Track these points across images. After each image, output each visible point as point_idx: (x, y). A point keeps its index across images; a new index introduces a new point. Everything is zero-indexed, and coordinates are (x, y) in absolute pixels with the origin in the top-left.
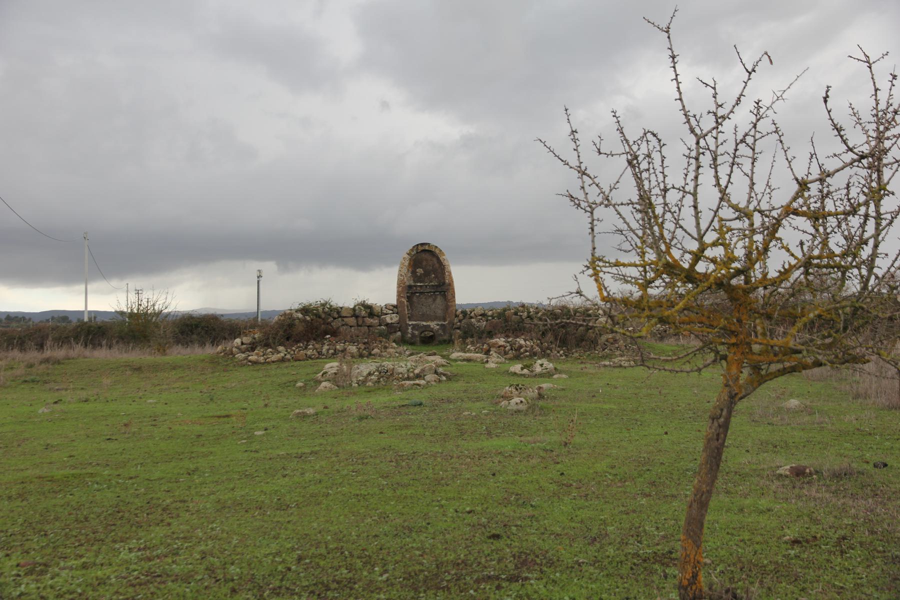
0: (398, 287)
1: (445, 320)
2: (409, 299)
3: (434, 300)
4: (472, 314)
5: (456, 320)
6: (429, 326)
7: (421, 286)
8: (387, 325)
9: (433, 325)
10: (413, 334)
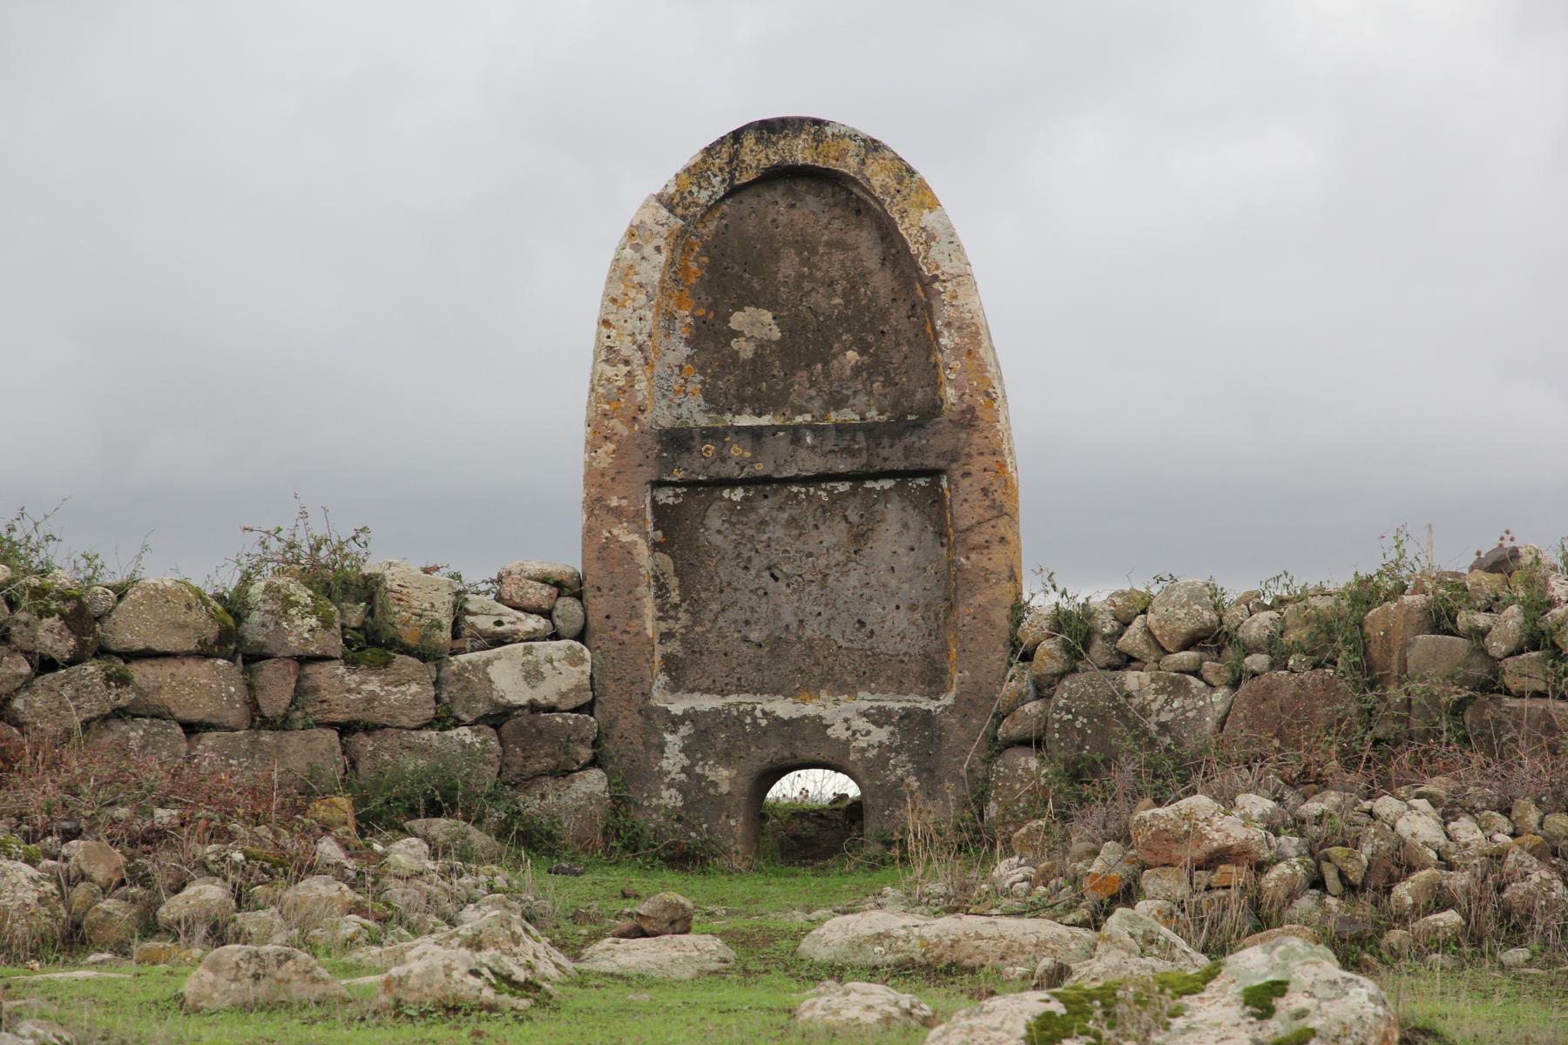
0: (598, 434)
1: (934, 680)
2: (672, 528)
3: (860, 538)
5: (1018, 681)
6: (819, 725)
7: (756, 434)
8: (499, 717)
10: (695, 789)
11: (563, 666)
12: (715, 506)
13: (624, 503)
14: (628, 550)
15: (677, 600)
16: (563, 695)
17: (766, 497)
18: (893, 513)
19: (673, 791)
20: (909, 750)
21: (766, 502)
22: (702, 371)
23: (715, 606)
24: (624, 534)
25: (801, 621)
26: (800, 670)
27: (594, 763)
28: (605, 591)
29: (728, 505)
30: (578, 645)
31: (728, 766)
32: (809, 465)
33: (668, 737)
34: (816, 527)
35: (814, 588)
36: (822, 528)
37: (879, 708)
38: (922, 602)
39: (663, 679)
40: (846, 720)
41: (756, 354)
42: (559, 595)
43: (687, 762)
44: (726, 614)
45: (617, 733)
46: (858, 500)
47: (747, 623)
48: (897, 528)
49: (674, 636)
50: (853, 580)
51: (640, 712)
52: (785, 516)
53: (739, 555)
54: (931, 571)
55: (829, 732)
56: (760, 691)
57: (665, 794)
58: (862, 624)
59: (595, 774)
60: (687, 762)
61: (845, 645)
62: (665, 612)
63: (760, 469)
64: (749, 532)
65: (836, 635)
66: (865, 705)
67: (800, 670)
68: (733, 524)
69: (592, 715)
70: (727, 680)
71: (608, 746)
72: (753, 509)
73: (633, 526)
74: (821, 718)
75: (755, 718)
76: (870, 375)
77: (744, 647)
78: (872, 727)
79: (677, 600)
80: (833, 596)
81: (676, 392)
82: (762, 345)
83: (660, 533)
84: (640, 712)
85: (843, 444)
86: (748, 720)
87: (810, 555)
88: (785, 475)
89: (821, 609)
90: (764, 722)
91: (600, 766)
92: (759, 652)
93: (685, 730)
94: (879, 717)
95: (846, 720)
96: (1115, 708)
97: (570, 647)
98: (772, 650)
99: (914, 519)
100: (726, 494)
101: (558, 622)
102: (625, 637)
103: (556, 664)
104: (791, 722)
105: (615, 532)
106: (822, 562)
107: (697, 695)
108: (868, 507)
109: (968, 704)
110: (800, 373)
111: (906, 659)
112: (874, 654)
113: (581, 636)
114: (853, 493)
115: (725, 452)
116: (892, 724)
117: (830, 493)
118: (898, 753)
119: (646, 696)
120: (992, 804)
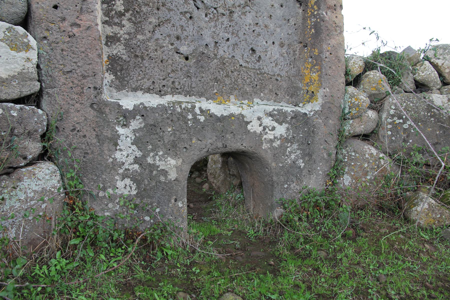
1: (294, 95)
4: (427, 73)
6: (242, 121)
9: (260, 119)
10: (147, 179)
15: (121, 8)
19: (128, 181)
20: (298, 141)
23: (153, 20)
25: (216, 43)
26: (216, 80)
27: (44, 156)
30: (20, 30)
31: (175, 156)
33: (121, 131)
35: (225, 19)
37: (278, 110)
38: (287, 42)
39: (109, 77)
40: (259, 119)
43: (139, 154)
44: (162, 28)
45: (68, 125)
47: (178, 38)
49: (119, 40)
50: (249, 19)
51: (92, 106)
54: (292, 22)
55: (249, 127)
56: (188, 93)
57: (120, 184)
58: (253, 50)
59: (46, 169)
60: (139, 154)
61: (244, 64)
62: (111, 17)
65: (238, 57)
66: (270, 109)
67: (216, 80)
69: (38, 106)
70: (164, 83)
71: (59, 140)
74: (243, 116)
75: (195, 115)
77: (177, 56)
78: (276, 124)
79: (121, 8)
80: (236, 28)
84: (92, 106)
89: (230, 36)
90: (202, 119)
91: (50, 159)
93: (136, 124)
94: (279, 117)
95: (259, 119)
96: (431, 116)
98: (198, 61)
102: (75, 30)
107: (139, 93)
111: (279, 78)
116: (287, 122)
119: (98, 90)
120: (346, 176)
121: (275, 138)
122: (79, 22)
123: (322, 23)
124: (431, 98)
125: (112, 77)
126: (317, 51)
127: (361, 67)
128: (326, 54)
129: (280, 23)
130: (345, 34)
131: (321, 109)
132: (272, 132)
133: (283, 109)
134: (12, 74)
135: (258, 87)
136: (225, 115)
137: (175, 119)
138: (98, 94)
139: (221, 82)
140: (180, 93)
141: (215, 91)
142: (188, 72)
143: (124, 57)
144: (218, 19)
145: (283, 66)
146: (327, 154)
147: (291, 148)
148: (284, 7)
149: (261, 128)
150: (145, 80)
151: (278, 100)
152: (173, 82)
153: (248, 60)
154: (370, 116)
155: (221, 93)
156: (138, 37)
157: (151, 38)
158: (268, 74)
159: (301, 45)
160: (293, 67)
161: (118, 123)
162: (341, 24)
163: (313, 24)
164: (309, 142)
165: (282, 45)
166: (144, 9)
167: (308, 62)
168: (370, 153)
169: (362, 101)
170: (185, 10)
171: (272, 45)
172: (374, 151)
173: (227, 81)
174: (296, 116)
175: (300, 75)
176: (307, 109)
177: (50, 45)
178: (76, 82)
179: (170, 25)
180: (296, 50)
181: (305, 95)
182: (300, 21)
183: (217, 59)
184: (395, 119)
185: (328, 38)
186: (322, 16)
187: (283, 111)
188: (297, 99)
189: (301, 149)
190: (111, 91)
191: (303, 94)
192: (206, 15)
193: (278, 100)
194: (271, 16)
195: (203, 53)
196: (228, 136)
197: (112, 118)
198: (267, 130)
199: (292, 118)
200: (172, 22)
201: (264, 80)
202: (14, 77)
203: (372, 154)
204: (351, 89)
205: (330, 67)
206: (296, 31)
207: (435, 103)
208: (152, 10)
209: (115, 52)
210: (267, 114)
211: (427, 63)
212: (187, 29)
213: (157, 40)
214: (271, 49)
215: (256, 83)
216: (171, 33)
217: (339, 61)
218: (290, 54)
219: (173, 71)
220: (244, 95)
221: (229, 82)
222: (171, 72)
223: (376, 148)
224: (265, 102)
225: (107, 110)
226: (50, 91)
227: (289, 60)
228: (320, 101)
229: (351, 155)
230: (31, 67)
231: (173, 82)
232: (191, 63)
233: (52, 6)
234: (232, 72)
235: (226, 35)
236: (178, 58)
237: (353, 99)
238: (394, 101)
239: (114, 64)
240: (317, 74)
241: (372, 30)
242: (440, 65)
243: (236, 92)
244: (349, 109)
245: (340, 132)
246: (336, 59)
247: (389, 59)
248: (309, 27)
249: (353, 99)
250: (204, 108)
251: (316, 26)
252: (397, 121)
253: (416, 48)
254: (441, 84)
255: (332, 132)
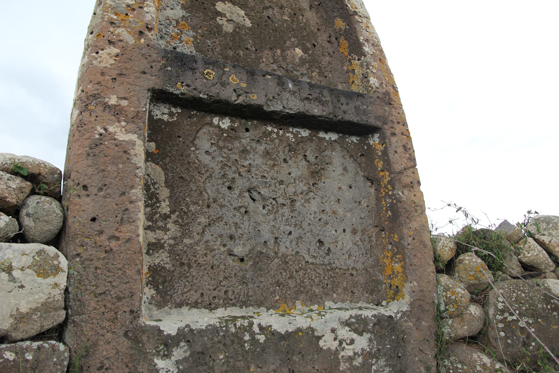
3: (316, 173)
4: (533, 252)
5: (456, 288)
6: (311, 337)
11: (29, 278)
12: (204, 130)
13: (124, 103)
14: (125, 150)
15: (167, 210)
16: (21, 318)
17: (247, 130)
18: (337, 159)
20: (385, 355)
21: (247, 134)
22: (194, 28)
23: (203, 220)
24: (121, 133)
25: (276, 238)
26: (278, 284)
28: (93, 190)
29: (216, 131)
30: (51, 250)
32: (291, 104)
34: (285, 161)
35: (286, 210)
36: (290, 162)
37: (358, 317)
38: (360, 228)
39: (149, 292)
40: (333, 331)
41: (234, 31)
42: (33, 192)
46: (313, 145)
47: (231, 237)
48: (340, 170)
49: (162, 247)
50: (314, 206)
51: (126, 334)
52: (262, 148)
53: (224, 176)
54: (364, 204)
55: (321, 343)
56: (244, 304)
58: (320, 242)
61: (311, 260)
62: (154, 222)
63: (255, 99)
64: (234, 157)
65: (303, 253)
66: (345, 315)
67: (278, 284)
68: (221, 148)
69: (60, 339)
70: (215, 293)
72: (237, 138)
73: (131, 126)
74: (313, 330)
75: (253, 334)
76: (311, 66)
77: (230, 260)
78: (355, 336)
79: (167, 210)
80: (299, 218)
81: (173, 38)
82: (239, 27)
83: (153, 145)
84: (126, 334)
85: (315, 95)
86: (247, 337)
87: (281, 183)
88: (272, 109)
89: (292, 229)
90: (262, 338)
92: (243, 265)
93: (179, 353)
94: (358, 325)
95: (333, 331)
97: (40, 253)
98: (255, 264)
99: (351, 166)
100: (216, 120)
101: (28, 222)
102: (113, 244)
103: (16, 273)
104: (288, 336)
105: (111, 129)
106: (291, 190)
107: (185, 309)
108: (321, 150)
109: (417, 308)
110: (266, 52)
111: (354, 273)
112: (332, 269)
113: (56, 240)
114: (310, 139)
115: (224, 78)
116: (368, 331)
117: (295, 136)
118: (378, 359)
119: (135, 314)
121: (355, 354)
122: (117, 234)
123: (399, 205)
124: (546, 285)
125: (153, 292)
126: (396, 236)
127: (452, 249)
128: (408, 240)
129: (350, 206)
130: (428, 212)
131: (409, 309)
132: (351, 347)
133: (362, 314)
134: (34, 306)
135: (329, 286)
136: (290, 330)
137: (228, 342)
138: (135, 318)
139: (284, 286)
140: (234, 305)
141: (277, 297)
142: (244, 277)
143: (167, 266)
144: (278, 211)
145: (357, 257)
146: (424, 368)
147: (376, 365)
148: (353, 188)
149: (337, 342)
150: (192, 292)
151: (355, 300)
152: (226, 292)
153: (315, 255)
154: (473, 313)
155: (284, 299)
156: (185, 241)
157: (200, 241)
158: (341, 269)
159: (377, 229)
160: (371, 256)
161: (158, 354)
162: (421, 203)
163: (388, 205)
164: (400, 355)
165: (354, 232)
166: (193, 208)
167: (388, 250)
168: (482, 363)
169: (460, 295)
170: (240, 204)
171: (343, 234)
172: (486, 360)
173: (292, 284)
174: (380, 320)
175: (379, 265)
176: (393, 309)
177: (82, 263)
178: (109, 305)
179: (222, 223)
180: (372, 236)
181: (388, 290)
182: (373, 202)
183: (277, 257)
184: (506, 315)
185: (408, 221)
186: (398, 196)
187: (363, 317)
188: (378, 295)
189: (390, 366)
190: (150, 310)
191: (386, 289)
192: (264, 207)
193: (355, 300)
194: (339, 199)
195: (262, 253)
196: (295, 358)
197: (150, 348)
198: (344, 344)
199: (374, 325)
200: (225, 220)
201: (336, 277)
202: (36, 310)
203: (484, 365)
204: (444, 279)
205: (415, 255)
206: (370, 214)
207: (553, 291)
208: (201, 209)
209: (157, 262)
210: (343, 323)
211: (530, 240)
212: (241, 226)
213: (207, 242)
214: (342, 239)
215: (326, 282)
216: (223, 232)
217: (425, 246)
218: (365, 241)
219: (225, 278)
220: (313, 299)
221: (294, 284)
222: (224, 279)
223: (489, 355)
224: (339, 305)
225: (145, 338)
226: (77, 318)
227: (364, 248)
228: (407, 298)
229: (457, 368)
230: (58, 294)
231: (226, 292)
232: (248, 267)
233: (90, 219)
234: (297, 271)
235: (288, 228)
236: (231, 262)
237: (448, 293)
238: (499, 295)
239: (157, 277)
240: (400, 265)
241: (459, 205)
242: (547, 243)
243: (303, 296)
244: (446, 306)
245: (438, 337)
246: (420, 244)
247: (484, 238)
248: (384, 208)
249: (448, 293)
250: (264, 324)
251: (393, 208)
252: (510, 318)
253: (513, 221)
254: (554, 266)
255: (427, 338)
